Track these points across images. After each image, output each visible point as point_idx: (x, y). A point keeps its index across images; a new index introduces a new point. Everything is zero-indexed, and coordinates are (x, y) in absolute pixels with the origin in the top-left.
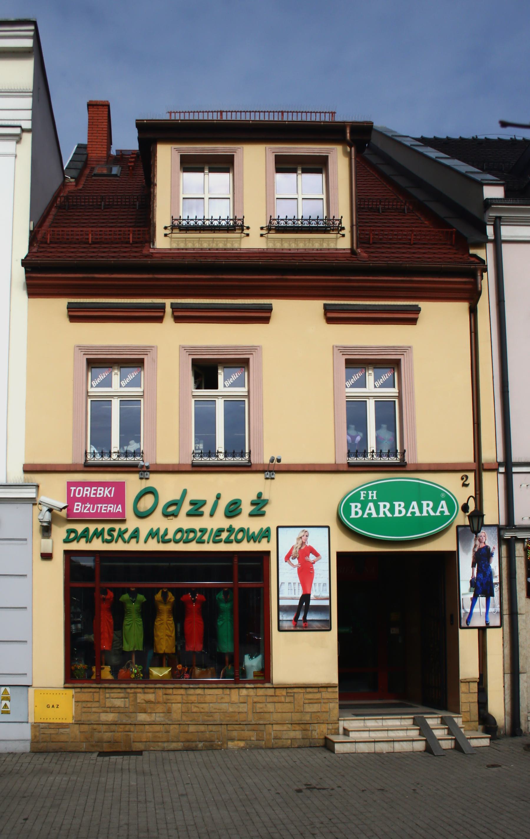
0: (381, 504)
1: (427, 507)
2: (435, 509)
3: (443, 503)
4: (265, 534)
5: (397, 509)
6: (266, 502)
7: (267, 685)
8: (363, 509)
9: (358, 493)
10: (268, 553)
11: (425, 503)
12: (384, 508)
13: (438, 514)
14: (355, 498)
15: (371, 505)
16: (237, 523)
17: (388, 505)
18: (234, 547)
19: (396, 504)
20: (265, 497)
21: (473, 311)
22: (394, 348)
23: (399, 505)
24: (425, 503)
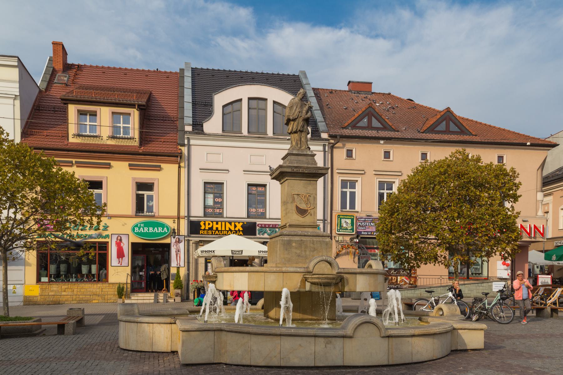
0: (145, 228)
1: (160, 229)
2: (163, 230)
3: (165, 228)
4: (107, 236)
5: (150, 230)
6: (108, 227)
7: (107, 283)
8: (139, 229)
9: (138, 225)
10: (108, 242)
11: (159, 228)
12: (146, 230)
13: (164, 231)
14: (136, 226)
15: (142, 228)
17: (147, 228)
19: (150, 228)
20: (108, 225)
22: (152, 179)
23: (151, 229)
24: (159, 228)
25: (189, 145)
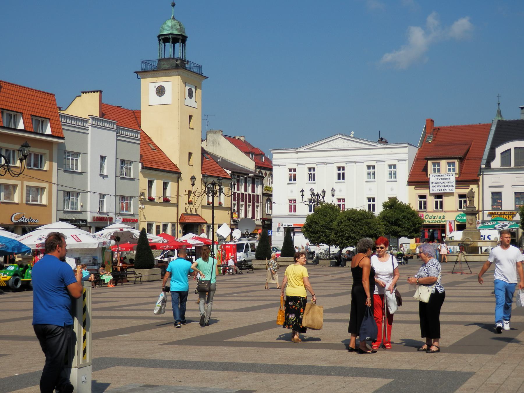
4: (445, 221)
12: (463, 217)
14: (458, 216)
16: (440, 220)
18: (440, 223)
21: (479, 187)
25: (483, 175)
